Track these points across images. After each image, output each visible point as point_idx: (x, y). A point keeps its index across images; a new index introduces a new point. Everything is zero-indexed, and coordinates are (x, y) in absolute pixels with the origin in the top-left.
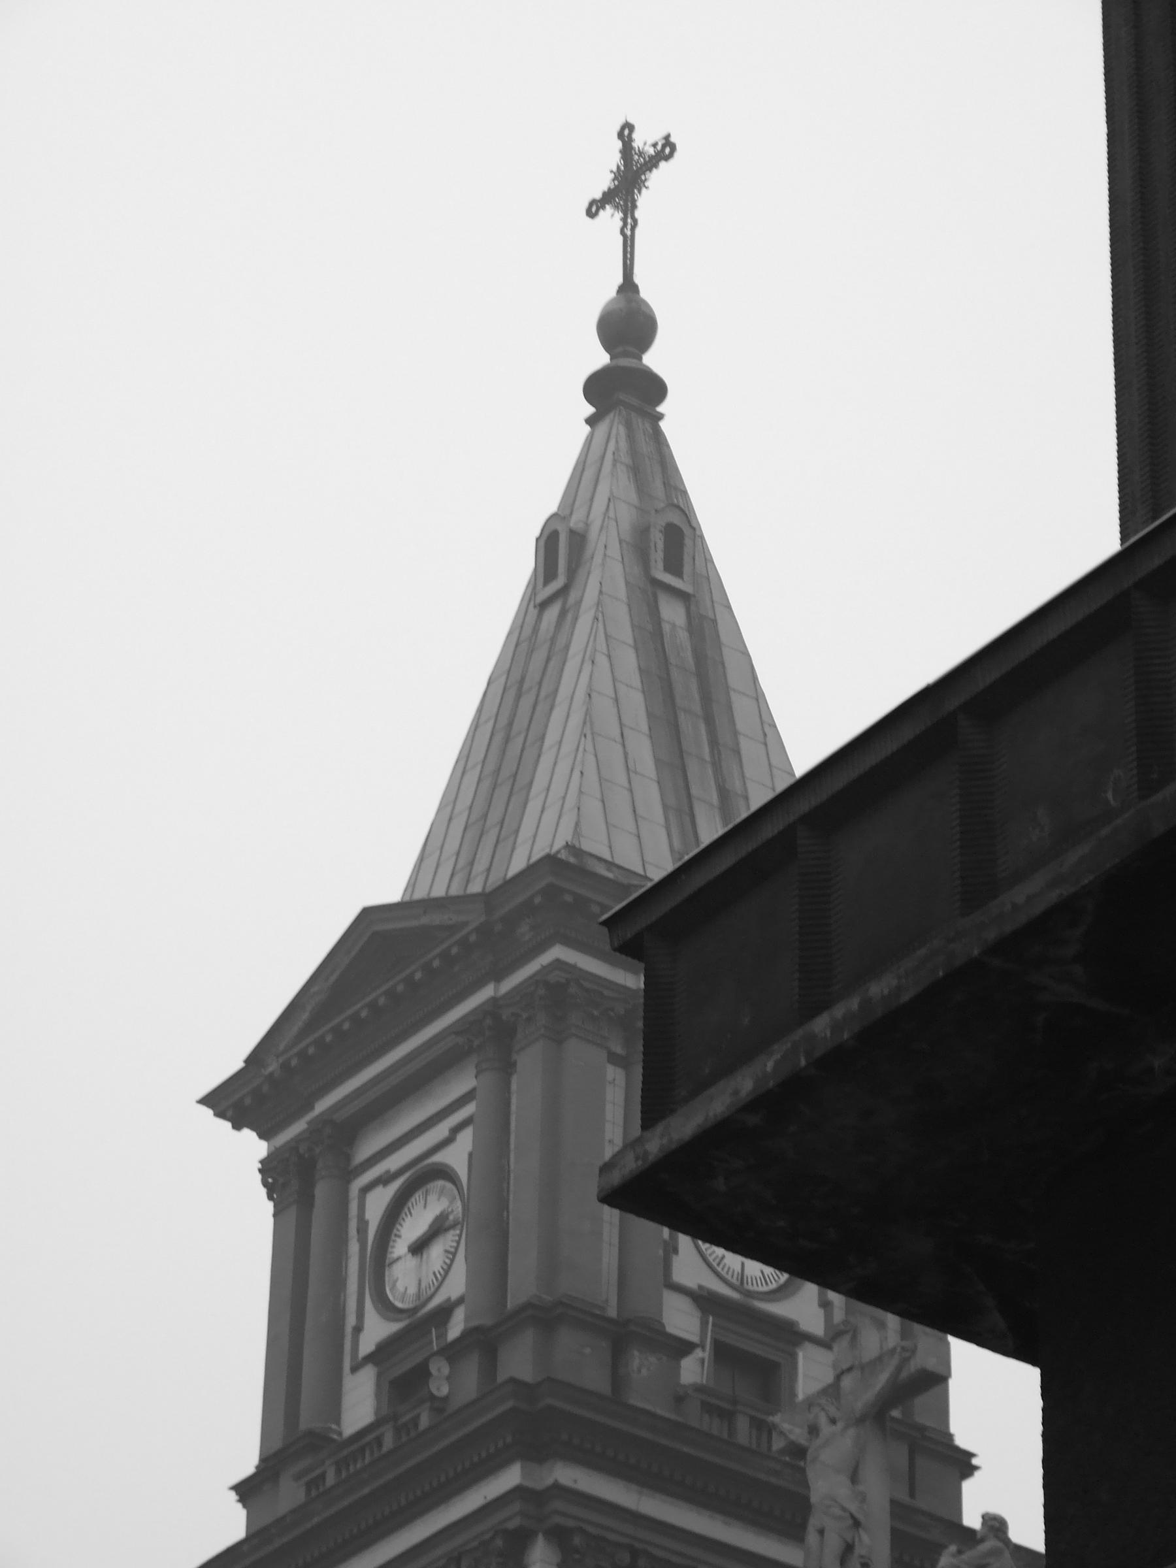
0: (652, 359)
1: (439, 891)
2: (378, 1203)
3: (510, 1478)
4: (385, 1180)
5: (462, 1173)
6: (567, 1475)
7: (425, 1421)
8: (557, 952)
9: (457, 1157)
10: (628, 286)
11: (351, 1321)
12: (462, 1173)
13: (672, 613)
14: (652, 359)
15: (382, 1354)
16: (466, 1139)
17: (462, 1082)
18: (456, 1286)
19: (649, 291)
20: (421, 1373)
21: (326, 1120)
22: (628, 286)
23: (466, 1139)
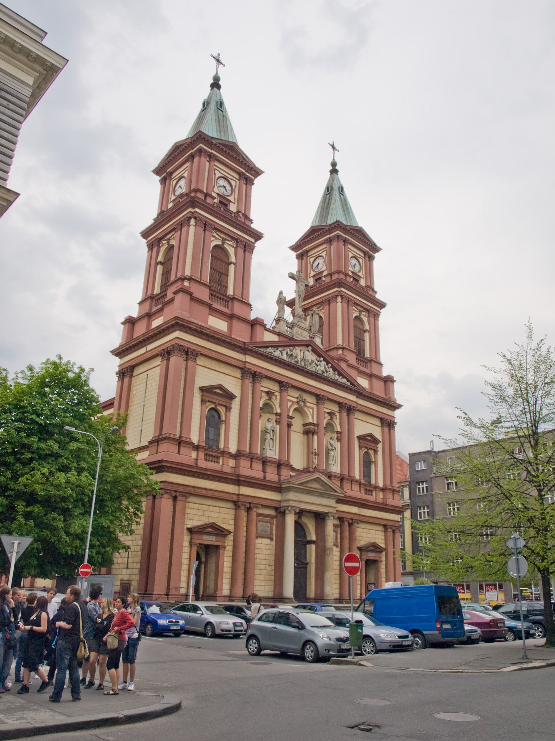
0: (337, 168)
1: (317, 224)
2: (312, 260)
3: (336, 289)
4: (313, 257)
5: (324, 256)
6: (342, 289)
7: (323, 283)
8: (338, 232)
9: (324, 254)
10: (334, 160)
11: (309, 273)
12: (324, 255)
13: (342, 196)
14: (337, 168)
15: (314, 276)
16: (325, 253)
17: (325, 246)
18: (324, 268)
19: (336, 160)
20: (320, 278)
21: (306, 250)
22: (334, 160)
23: (325, 253)
